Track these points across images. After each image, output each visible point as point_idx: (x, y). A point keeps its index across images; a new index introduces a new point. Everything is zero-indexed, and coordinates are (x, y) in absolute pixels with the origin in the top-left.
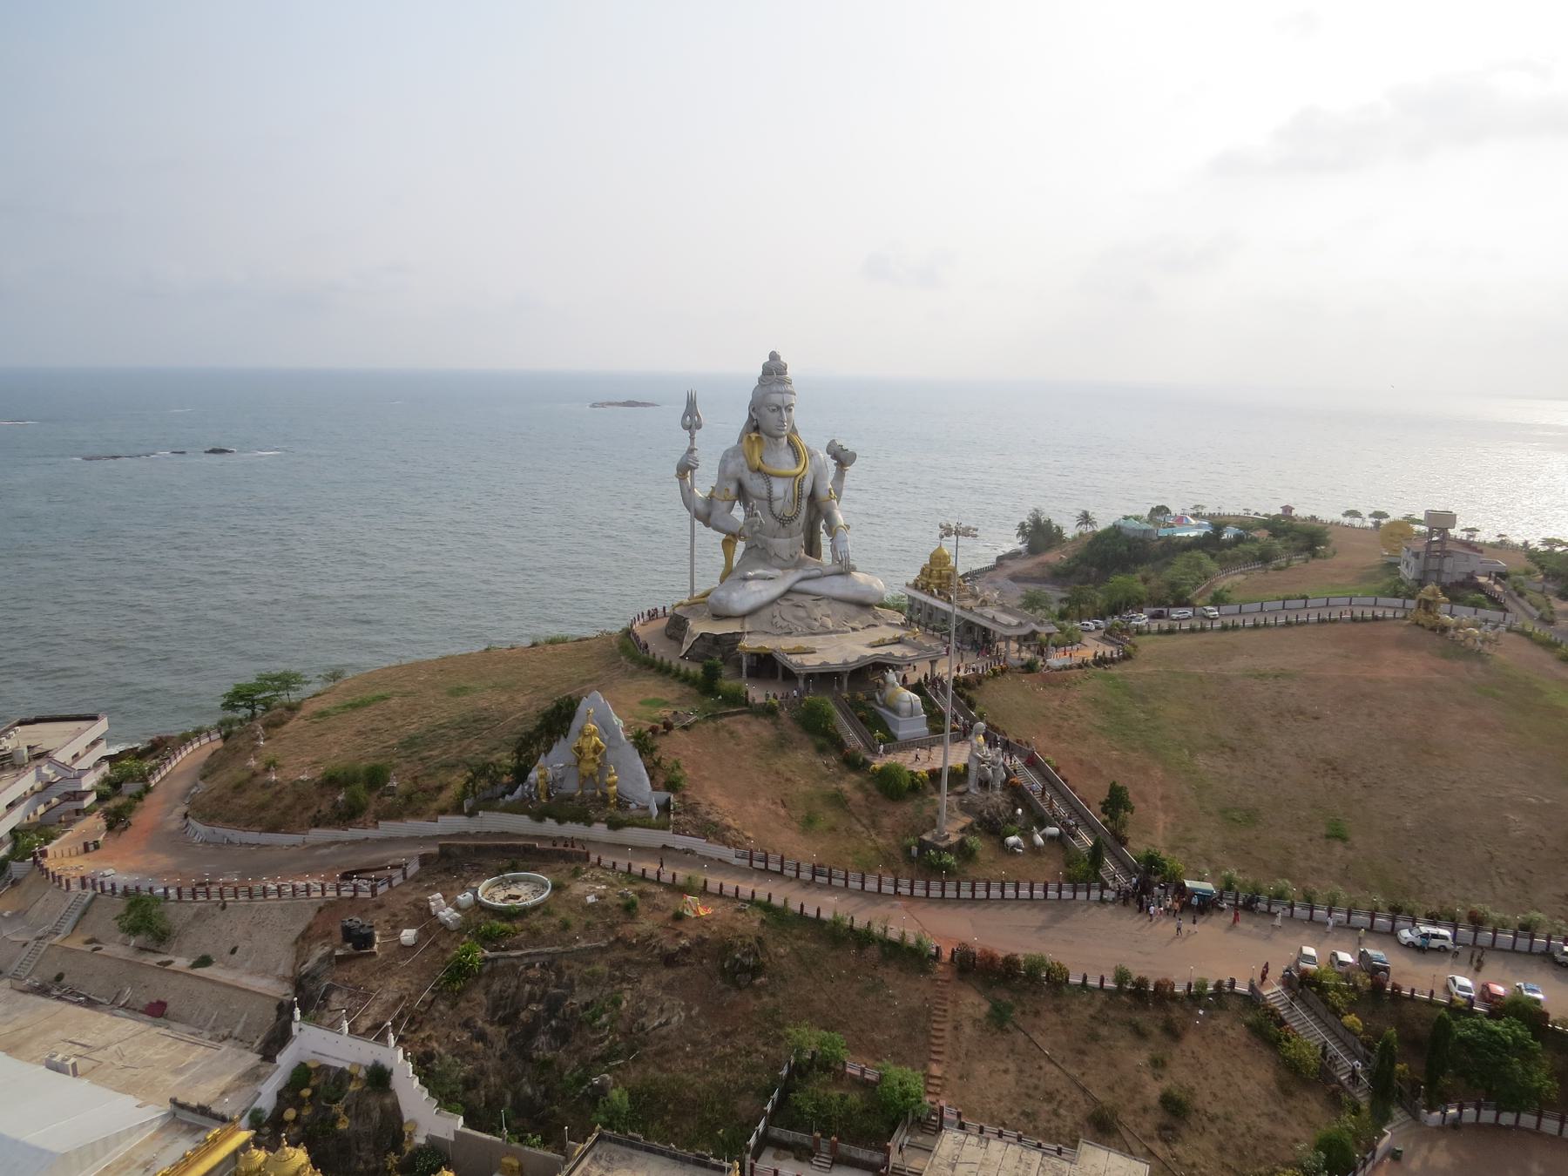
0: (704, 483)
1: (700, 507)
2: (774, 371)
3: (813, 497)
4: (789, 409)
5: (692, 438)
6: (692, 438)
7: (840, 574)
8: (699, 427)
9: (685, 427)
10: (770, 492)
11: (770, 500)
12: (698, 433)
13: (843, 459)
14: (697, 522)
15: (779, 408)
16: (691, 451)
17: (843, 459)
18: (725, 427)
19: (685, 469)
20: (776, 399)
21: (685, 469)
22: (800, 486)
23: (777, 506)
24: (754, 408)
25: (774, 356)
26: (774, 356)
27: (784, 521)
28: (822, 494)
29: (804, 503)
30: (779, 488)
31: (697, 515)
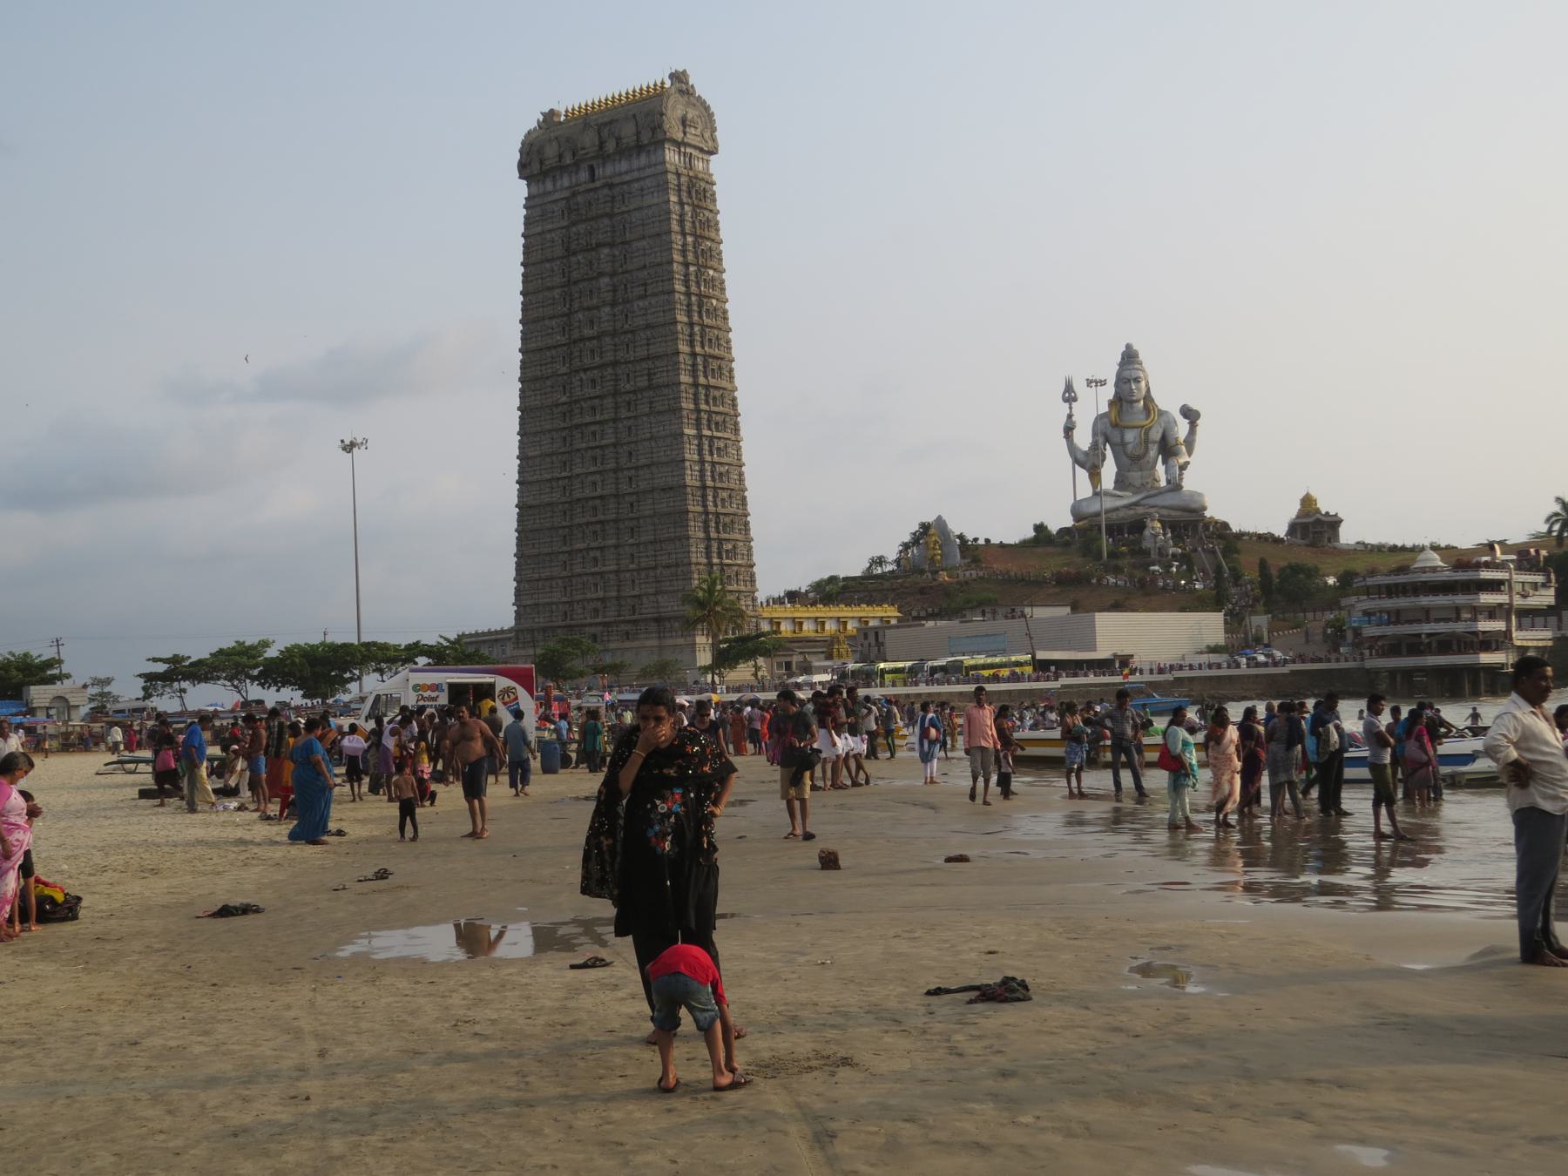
0: (1083, 439)
1: (1081, 457)
2: (1129, 357)
4: (1137, 380)
8: (1075, 399)
9: (1066, 400)
11: (1123, 444)
13: (1190, 414)
16: (1070, 416)
18: (1094, 404)
19: (1069, 430)
20: (1126, 374)
21: (1069, 430)
25: (1128, 346)
26: (1128, 346)
30: (1130, 436)
31: (1076, 461)
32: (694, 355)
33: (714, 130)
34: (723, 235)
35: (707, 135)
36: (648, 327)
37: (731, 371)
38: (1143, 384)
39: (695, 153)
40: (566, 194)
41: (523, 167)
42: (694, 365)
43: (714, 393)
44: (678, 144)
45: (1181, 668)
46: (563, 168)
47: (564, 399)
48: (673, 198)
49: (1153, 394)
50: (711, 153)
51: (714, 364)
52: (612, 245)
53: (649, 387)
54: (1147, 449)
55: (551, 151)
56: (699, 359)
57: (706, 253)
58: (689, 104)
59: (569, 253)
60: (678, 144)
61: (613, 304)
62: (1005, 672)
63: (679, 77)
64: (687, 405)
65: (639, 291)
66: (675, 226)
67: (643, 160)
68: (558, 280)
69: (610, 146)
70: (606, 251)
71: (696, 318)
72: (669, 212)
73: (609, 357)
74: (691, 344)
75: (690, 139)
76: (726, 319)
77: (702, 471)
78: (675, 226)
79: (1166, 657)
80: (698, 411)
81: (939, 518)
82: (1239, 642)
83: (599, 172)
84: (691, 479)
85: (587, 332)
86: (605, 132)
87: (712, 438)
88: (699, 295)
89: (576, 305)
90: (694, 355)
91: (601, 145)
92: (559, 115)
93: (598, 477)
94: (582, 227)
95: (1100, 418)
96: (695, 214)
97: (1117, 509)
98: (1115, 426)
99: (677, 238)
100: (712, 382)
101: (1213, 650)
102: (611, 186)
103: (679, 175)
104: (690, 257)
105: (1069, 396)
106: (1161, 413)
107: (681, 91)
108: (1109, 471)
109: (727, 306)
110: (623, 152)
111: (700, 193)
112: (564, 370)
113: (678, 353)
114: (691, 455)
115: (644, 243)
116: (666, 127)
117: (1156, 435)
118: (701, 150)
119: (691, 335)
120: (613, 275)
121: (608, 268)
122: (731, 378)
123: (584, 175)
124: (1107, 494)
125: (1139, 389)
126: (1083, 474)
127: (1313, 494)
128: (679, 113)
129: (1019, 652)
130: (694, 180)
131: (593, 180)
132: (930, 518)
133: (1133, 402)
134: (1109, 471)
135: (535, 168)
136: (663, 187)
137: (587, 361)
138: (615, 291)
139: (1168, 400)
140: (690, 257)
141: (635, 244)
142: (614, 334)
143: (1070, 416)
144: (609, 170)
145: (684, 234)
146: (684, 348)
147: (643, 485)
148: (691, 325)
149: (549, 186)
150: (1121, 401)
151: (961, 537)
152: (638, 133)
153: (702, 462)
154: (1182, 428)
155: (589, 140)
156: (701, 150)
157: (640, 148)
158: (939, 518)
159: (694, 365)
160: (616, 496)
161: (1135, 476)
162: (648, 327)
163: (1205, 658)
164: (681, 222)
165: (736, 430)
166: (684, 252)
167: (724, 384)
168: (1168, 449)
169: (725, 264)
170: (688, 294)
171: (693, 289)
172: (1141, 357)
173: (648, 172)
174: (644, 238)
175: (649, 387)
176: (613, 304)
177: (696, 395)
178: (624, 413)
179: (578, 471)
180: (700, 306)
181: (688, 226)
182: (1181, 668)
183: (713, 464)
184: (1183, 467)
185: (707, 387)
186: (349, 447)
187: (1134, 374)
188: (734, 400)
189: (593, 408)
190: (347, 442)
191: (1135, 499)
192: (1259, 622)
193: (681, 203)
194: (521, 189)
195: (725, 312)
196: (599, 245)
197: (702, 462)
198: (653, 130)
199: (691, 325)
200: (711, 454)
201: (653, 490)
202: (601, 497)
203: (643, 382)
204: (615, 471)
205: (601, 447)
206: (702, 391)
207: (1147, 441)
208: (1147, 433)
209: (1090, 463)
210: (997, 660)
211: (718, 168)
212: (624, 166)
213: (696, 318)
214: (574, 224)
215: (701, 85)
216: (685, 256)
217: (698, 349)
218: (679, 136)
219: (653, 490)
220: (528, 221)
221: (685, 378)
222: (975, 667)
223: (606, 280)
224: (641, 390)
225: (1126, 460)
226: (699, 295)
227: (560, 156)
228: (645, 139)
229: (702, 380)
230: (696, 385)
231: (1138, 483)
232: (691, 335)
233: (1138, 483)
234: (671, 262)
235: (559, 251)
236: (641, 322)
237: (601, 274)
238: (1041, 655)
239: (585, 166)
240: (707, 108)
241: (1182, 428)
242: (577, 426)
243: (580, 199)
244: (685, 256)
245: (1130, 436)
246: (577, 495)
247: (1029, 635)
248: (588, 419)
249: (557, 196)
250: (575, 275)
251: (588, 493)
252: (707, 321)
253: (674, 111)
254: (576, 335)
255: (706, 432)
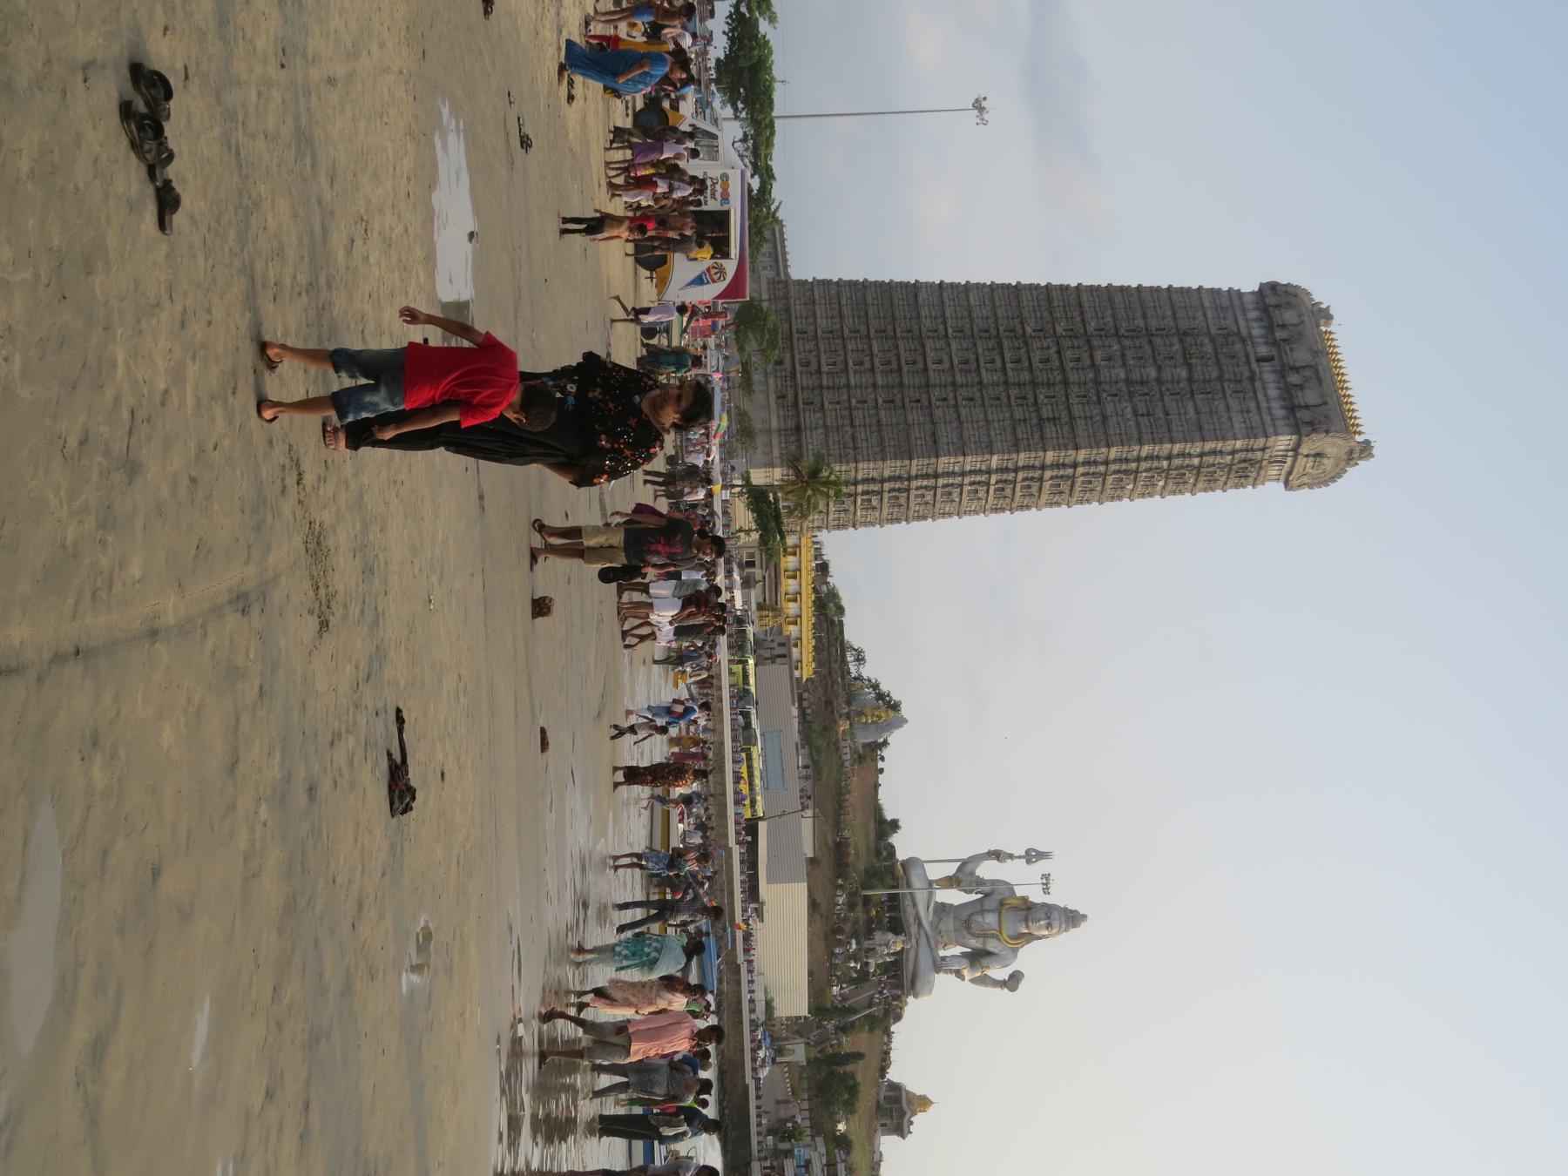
0: (987, 871)
1: (969, 867)
2: (1073, 918)
4: (1049, 926)
7: (934, 963)
8: (1029, 862)
9: (1028, 852)
11: (982, 912)
16: (1011, 856)
19: (997, 855)
20: (1055, 915)
21: (997, 855)
23: (978, 918)
25: (1084, 917)
28: (985, 962)
30: (991, 919)
31: (965, 863)
32: (1075, 465)
33: (1311, 486)
34: (1201, 495)
35: (1305, 479)
36: (1104, 418)
37: (1058, 504)
38: (1046, 933)
39: (1287, 467)
40: (1244, 332)
41: (1273, 287)
42: (1064, 466)
43: (1035, 486)
44: (1296, 449)
45: (750, 971)
46: (1270, 328)
47: (1029, 330)
48: (1239, 444)
49: (1035, 943)
50: (1286, 483)
51: (1065, 486)
52: (1190, 380)
53: (1041, 419)
55: (1289, 316)
56: (1070, 471)
57: (1180, 477)
58: (1338, 459)
59: (1183, 335)
60: (1296, 449)
61: (1128, 381)
62: (744, 788)
63: (1366, 449)
64: (1022, 458)
65: (1142, 409)
66: (1209, 446)
67: (1279, 413)
68: (1153, 323)
69: (1294, 378)
70: (1184, 374)
71: (1113, 467)
72: (1224, 439)
73: (1073, 377)
74: (1087, 463)
75: (1301, 461)
76: (1113, 498)
77: (953, 474)
78: (1209, 446)
79: (761, 953)
80: (1016, 470)
81: (905, 721)
82: (776, 1033)
83: (1267, 367)
84: (945, 463)
85: (1098, 355)
86: (1308, 373)
87: (988, 484)
88: (1137, 471)
89: (1127, 342)
90: (1075, 465)
91: (1296, 369)
92: (1327, 324)
93: (947, 365)
94: (1208, 348)
95: (1010, 887)
96: (1222, 467)
97: (915, 905)
98: (1002, 904)
99: (1197, 448)
100: (1047, 485)
101: (769, 1005)
102: (1252, 379)
103: (1263, 449)
104: (1177, 462)
105: (1033, 856)
106: (1015, 951)
107: (1351, 452)
108: (954, 897)
109: (1126, 501)
110: (1288, 392)
111: (1244, 471)
112: (1059, 330)
113: (1077, 448)
114: (970, 462)
115: (1191, 414)
116: (1314, 436)
117: (992, 945)
118: (1289, 473)
119: (1095, 463)
120: (1159, 380)
121: (1167, 375)
122: (1051, 505)
123: (1263, 350)
124: (931, 895)
125: (1040, 928)
126: (951, 869)
127: (931, 1109)
128: (1329, 450)
129: (766, 803)
130: (1258, 465)
131: (1260, 360)
132: (905, 711)
133: (1026, 920)
134: (954, 897)
135: (1271, 300)
136: (1250, 433)
137: (1069, 354)
138: (1142, 383)
139: (1029, 958)
140: (1177, 462)
141: (1190, 405)
142: (1097, 382)
143: (1011, 856)
144: (1269, 377)
145: (1201, 455)
146: (1082, 455)
147: (938, 413)
148: (1106, 463)
149: (1253, 314)
150: (1027, 909)
151: (885, 743)
152: (1307, 407)
153: (963, 474)
154: (999, 973)
155: (1300, 356)
156: (1289, 473)
157: (1292, 409)
158: (905, 721)
159: (1064, 466)
160: (928, 385)
161: (949, 924)
162: (1104, 418)
163: (760, 996)
164: (1214, 452)
165: (996, 510)
166: (1182, 455)
167: (1044, 497)
168: (977, 957)
169: (1170, 498)
170: (1138, 459)
171: (1144, 465)
172: (1073, 931)
173: (1267, 418)
174: (1198, 412)
175: (1041, 419)
176: (1128, 381)
177: (1033, 467)
178: (1013, 392)
179: (954, 345)
180: (1126, 472)
181: (1209, 459)
182: (750, 971)
183: (961, 486)
184: (958, 974)
185: (1041, 479)
186: (978, 106)
187: (1056, 924)
188: (1028, 507)
189: (1019, 361)
190: (984, 104)
191: (925, 924)
192: (798, 1053)
193: (1233, 453)
194: (1249, 285)
195: (1120, 498)
196: (1190, 367)
197: (963, 474)
198: (1311, 423)
199: (1106, 463)
200: (971, 484)
201: (933, 422)
202: (926, 369)
203: (1046, 412)
204: (954, 384)
205: (978, 369)
206: (1037, 474)
207: (985, 936)
208: (993, 936)
209: (962, 877)
210: (757, 781)
211: (1272, 489)
212: (1273, 392)
213: (1113, 467)
214: (1212, 340)
215: (1356, 474)
216: (1178, 456)
217: (1080, 470)
218: (1304, 450)
219: (933, 422)
220: (1215, 293)
221: (1050, 456)
222: (749, 758)
223: (1153, 374)
224: (1038, 411)
225: (965, 915)
226: (1137, 471)
227: (1283, 326)
228: (1303, 415)
229: (1048, 474)
230: (1043, 468)
231: (942, 927)
232: (1095, 463)
233: (942, 927)
234: (1172, 441)
235: (1184, 324)
236: (1109, 409)
237: (1159, 369)
238: (762, 826)
239: (1274, 352)
240: (1333, 479)
241: (999, 973)
242: (1000, 344)
243: (1239, 346)
244: (1178, 456)
245: (991, 919)
246: (929, 344)
247: (783, 814)
248: (1007, 355)
249: (1242, 323)
250: (1158, 341)
251: (931, 355)
252: (1110, 479)
253: (1331, 445)
254: (1096, 343)
255: (994, 478)
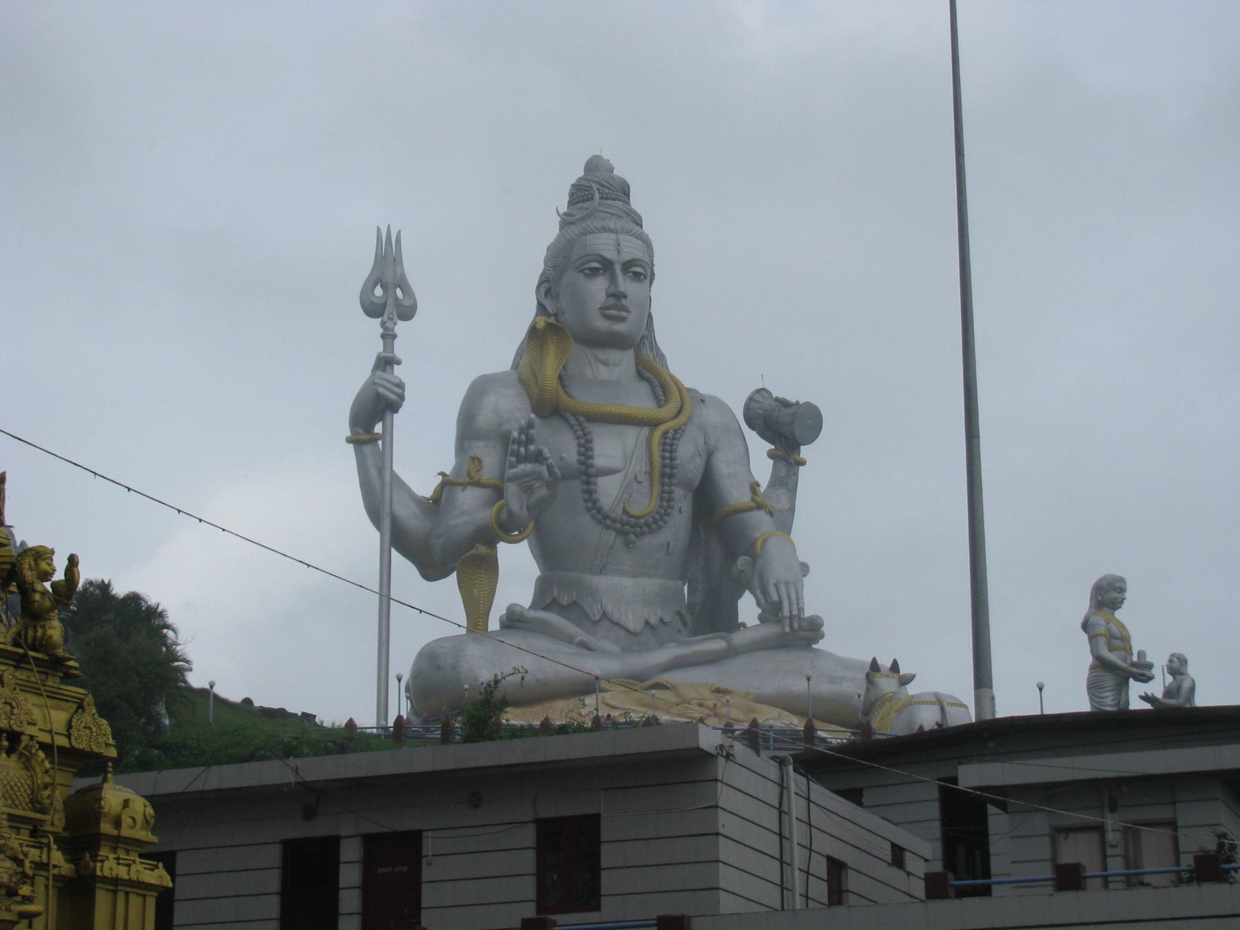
0: (424, 453)
1: (408, 513)
3: (705, 494)
5: (388, 337)
6: (388, 337)
8: (407, 313)
9: (372, 309)
10: (586, 450)
11: (586, 473)
12: (401, 327)
13: (787, 427)
14: (396, 555)
15: (607, 266)
16: (386, 362)
17: (787, 427)
18: (472, 334)
19: (374, 411)
21: (374, 411)
22: (669, 444)
23: (608, 490)
24: (549, 286)
27: (630, 528)
29: (683, 502)
30: (612, 448)
54: (666, 498)
95: (479, 390)
108: (518, 570)
134: (518, 570)
143: (386, 362)
154: (760, 458)
